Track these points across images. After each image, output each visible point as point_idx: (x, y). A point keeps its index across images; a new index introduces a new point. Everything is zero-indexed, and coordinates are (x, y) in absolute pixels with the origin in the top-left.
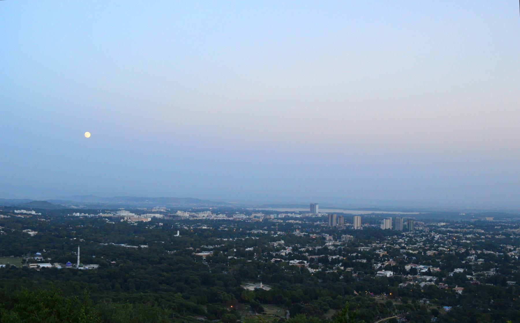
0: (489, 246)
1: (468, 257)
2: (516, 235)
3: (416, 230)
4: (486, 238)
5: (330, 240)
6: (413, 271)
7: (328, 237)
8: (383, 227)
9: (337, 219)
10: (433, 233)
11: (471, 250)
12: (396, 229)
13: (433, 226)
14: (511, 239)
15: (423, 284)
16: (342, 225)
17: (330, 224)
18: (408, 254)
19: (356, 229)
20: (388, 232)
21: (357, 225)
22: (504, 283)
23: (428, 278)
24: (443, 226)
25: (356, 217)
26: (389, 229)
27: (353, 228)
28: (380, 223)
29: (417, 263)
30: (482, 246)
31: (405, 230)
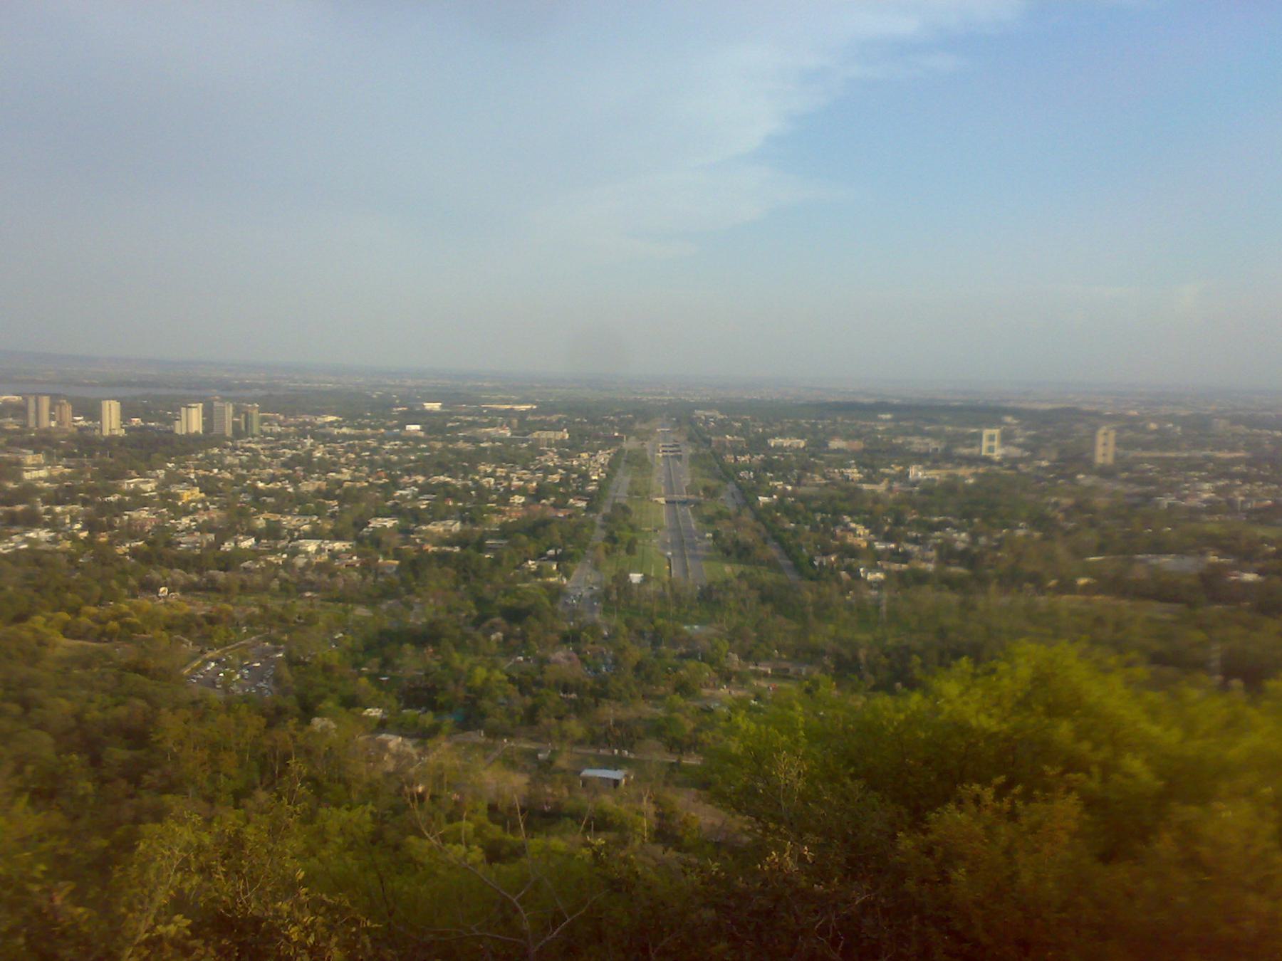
0: (443, 468)
1: (399, 493)
2: (493, 441)
3: (266, 434)
4: (430, 449)
5: (39, 467)
6: (273, 532)
7: (30, 458)
8: (180, 428)
9: (52, 409)
10: (309, 442)
11: (401, 476)
12: (216, 430)
13: (308, 424)
14: (485, 449)
15: (300, 561)
16: (66, 426)
17: (32, 424)
18: (257, 494)
19: (106, 433)
20: (190, 444)
21: (112, 421)
22: (480, 547)
23: (311, 546)
24: (331, 424)
25: (106, 404)
26: (197, 433)
27: (97, 432)
28: (170, 421)
29: (278, 510)
30: (424, 467)
31: (238, 434)
